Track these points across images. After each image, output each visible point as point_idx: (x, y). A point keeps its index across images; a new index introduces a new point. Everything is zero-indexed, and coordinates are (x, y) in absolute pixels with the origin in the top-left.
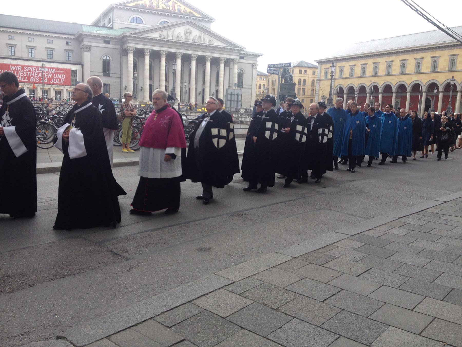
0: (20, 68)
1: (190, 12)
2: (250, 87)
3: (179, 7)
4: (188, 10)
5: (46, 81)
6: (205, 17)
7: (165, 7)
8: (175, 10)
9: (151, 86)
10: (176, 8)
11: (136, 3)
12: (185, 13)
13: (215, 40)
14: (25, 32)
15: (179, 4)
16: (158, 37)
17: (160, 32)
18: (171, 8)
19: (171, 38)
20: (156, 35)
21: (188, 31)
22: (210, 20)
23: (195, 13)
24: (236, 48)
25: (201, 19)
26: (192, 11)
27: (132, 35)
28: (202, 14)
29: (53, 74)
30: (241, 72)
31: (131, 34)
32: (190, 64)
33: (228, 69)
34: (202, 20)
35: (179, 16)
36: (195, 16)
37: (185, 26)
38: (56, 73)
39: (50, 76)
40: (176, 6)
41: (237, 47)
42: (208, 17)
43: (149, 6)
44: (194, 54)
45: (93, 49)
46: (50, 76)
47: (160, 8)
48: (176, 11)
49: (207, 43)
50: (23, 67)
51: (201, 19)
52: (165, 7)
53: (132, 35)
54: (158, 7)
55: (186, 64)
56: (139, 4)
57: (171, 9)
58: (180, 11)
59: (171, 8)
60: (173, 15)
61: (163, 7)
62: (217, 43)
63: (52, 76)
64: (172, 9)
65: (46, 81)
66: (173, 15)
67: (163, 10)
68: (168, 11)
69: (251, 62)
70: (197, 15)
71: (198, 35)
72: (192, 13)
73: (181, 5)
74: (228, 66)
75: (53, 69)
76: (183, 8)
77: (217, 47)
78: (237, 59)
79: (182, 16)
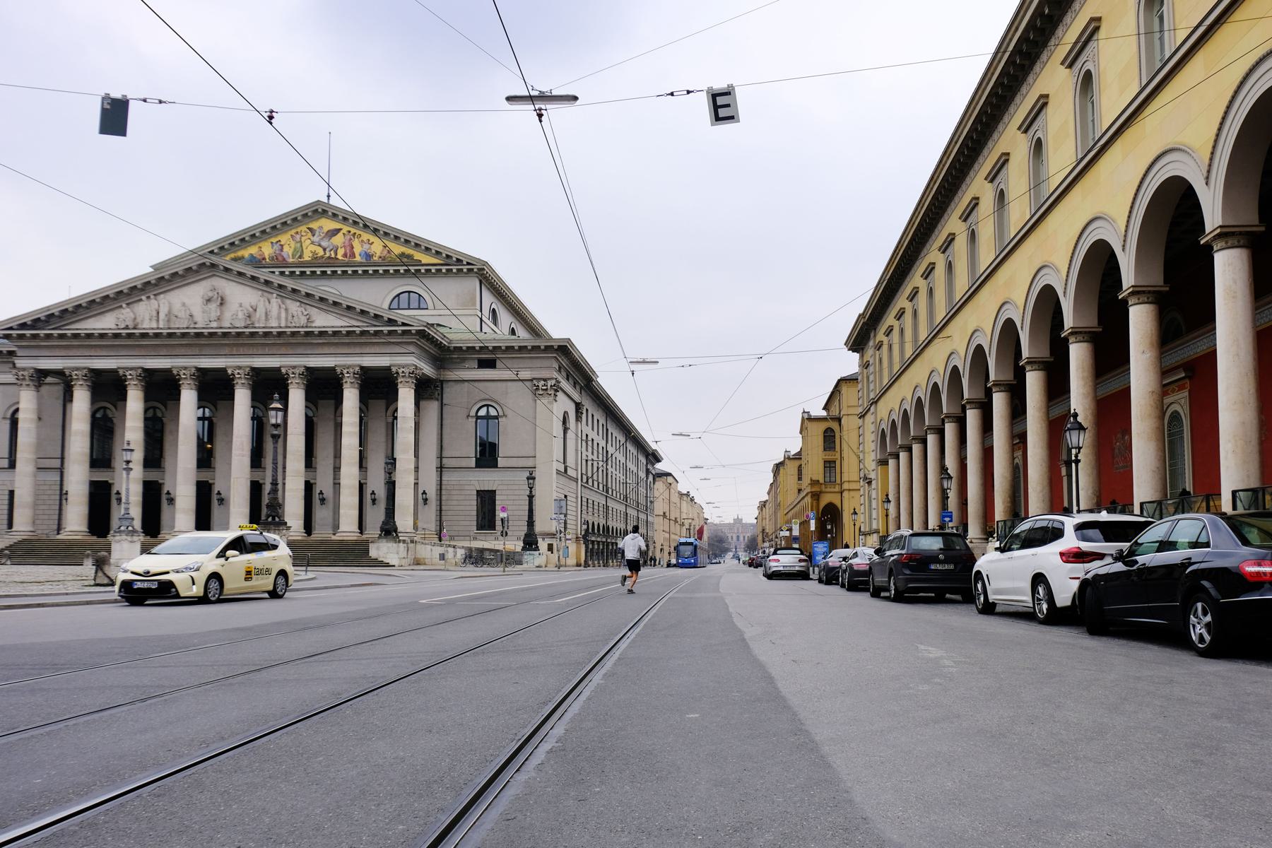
1: (403, 254)
2: (529, 463)
3: (366, 246)
4: (397, 249)
6: (449, 261)
7: (321, 252)
8: (353, 255)
10: (358, 249)
11: (232, 255)
15: (366, 236)
16: (113, 326)
17: (117, 312)
18: (341, 252)
19: (148, 325)
20: (106, 323)
21: (210, 294)
22: (465, 268)
23: (418, 256)
24: (386, 329)
25: (433, 269)
27: (13, 332)
28: (438, 253)
30: (493, 412)
31: (11, 328)
33: (432, 408)
36: (419, 263)
37: (204, 283)
40: (356, 243)
41: (391, 322)
42: (458, 260)
43: (272, 258)
47: (307, 257)
48: (358, 258)
49: (273, 324)
52: (321, 252)
53: (13, 332)
54: (301, 257)
55: (326, 407)
57: (339, 257)
58: (368, 256)
59: (341, 252)
60: (350, 270)
61: (314, 253)
62: (324, 321)
64: (345, 255)
67: (316, 261)
68: (332, 262)
70: (426, 259)
71: (247, 305)
72: (409, 257)
73: (373, 238)
74: (430, 398)
76: (378, 247)
77: (322, 334)
78: (400, 366)
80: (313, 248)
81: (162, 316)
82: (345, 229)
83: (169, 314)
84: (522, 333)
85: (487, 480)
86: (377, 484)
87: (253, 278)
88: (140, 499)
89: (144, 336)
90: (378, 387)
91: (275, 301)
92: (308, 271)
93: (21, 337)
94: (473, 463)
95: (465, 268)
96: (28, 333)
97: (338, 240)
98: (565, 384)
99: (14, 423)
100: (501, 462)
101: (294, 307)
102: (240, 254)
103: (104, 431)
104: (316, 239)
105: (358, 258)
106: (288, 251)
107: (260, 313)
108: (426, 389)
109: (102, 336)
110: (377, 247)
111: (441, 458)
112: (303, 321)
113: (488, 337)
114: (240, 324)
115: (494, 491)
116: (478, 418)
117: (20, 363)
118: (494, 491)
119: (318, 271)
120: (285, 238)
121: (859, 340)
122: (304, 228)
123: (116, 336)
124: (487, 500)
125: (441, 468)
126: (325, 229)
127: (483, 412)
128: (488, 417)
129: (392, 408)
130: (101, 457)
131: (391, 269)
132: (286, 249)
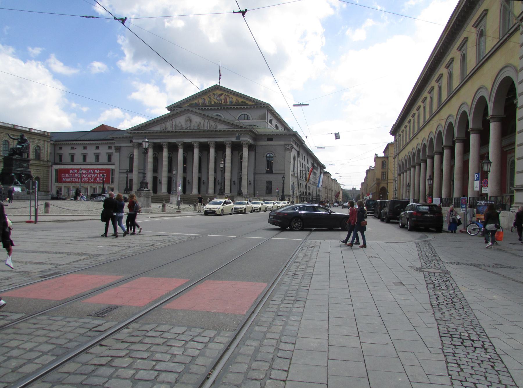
0: (76, 171)
1: (242, 102)
2: (283, 172)
3: (231, 99)
4: (240, 100)
5: (93, 180)
8: (227, 102)
9: (200, 179)
10: (228, 100)
12: (237, 104)
13: (218, 124)
14: (105, 142)
15: (231, 96)
18: (223, 101)
19: (169, 129)
20: (157, 128)
22: (262, 106)
23: (247, 102)
25: (252, 107)
26: (245, 101)
29: (97, 174)
30: (271, 155)
32: (224, 151)
33: (253, 154)
34: (257, 107)
35: (232, 107)
38: (100, 173)
39: (96, 176)
40: (228, 98)
41: (241, 127)
44: (195, 142)
45: (122, 149)
46: (96, 176)
47: (213, 103)
48: (228, 103)
50: (78, 170)
51: (252, 107)
52: (217, 101)
56: (193, 104)
58: (232, 102)
60: (226, 107)
61: (215, 102)
62: (221, 127)
63: (97, 176)
65: (93, 180)
66: (226, 107)
67: (216, 104)
68: (220, 105)
69: (282, 143)
70: (250, 103)
72: (245, 102)
75: (98, 169)
78: (244, 141)
79: (236, 107)
80: (214, 100)
81: (173, 126)
82: (225, 93)
83: (175, 125)
84: (280, 127)
85: (269, 177)
86: (235, 179)
87: (200, 113)
88: (167, 182)
89: (168, 132)
90: (237, 148)
91: (206, 121)
92: (213, 108)
93: (134, 133)
94: (265, 172)
95: (262, 106)
96: (136, 132)
97: (222, 97)
98: (295, 146)
99: (131, 159)
100: (274, 171)
101: (212, 123)
102: (192, 102)
103: (156, 161)
104: (215, 97)
105: (228, 103)
106: (207, 101)
107: (202, 124)
108: (251, 148)
109: (157, 132)
110: (234, 100)
111: (255, 170)
112: (215, 127)
113: (271, 131)
114: (196, 128)
115: (271, 181)
116: (267, 157)
117: (134, 141)
118: (271, 181)
119: (216, 108)
120: (206, 97)
121: (394, 131)
122: (212, 94)
123: (161, 132)
124: (269, 183)
125: (255, 173)
126: (218, 94)
127: (268, 155)
128: (270, 157)
129: (240, 154)
130: (155, 170)
131: (239, 107)
132: (206, 101)
